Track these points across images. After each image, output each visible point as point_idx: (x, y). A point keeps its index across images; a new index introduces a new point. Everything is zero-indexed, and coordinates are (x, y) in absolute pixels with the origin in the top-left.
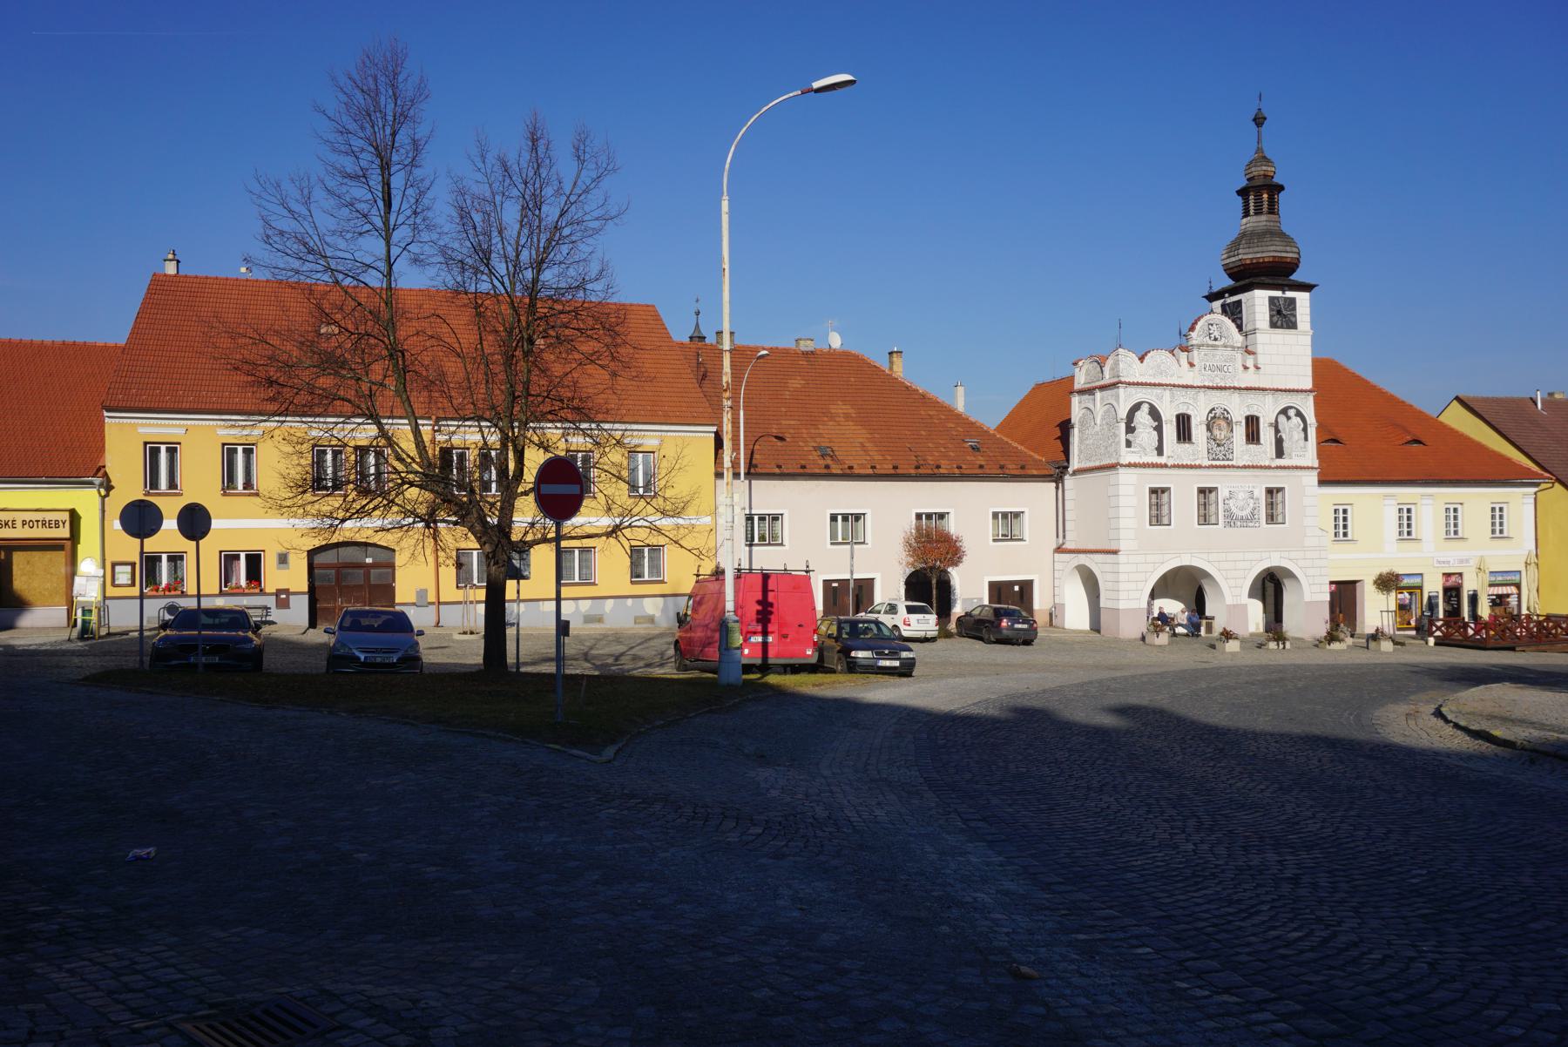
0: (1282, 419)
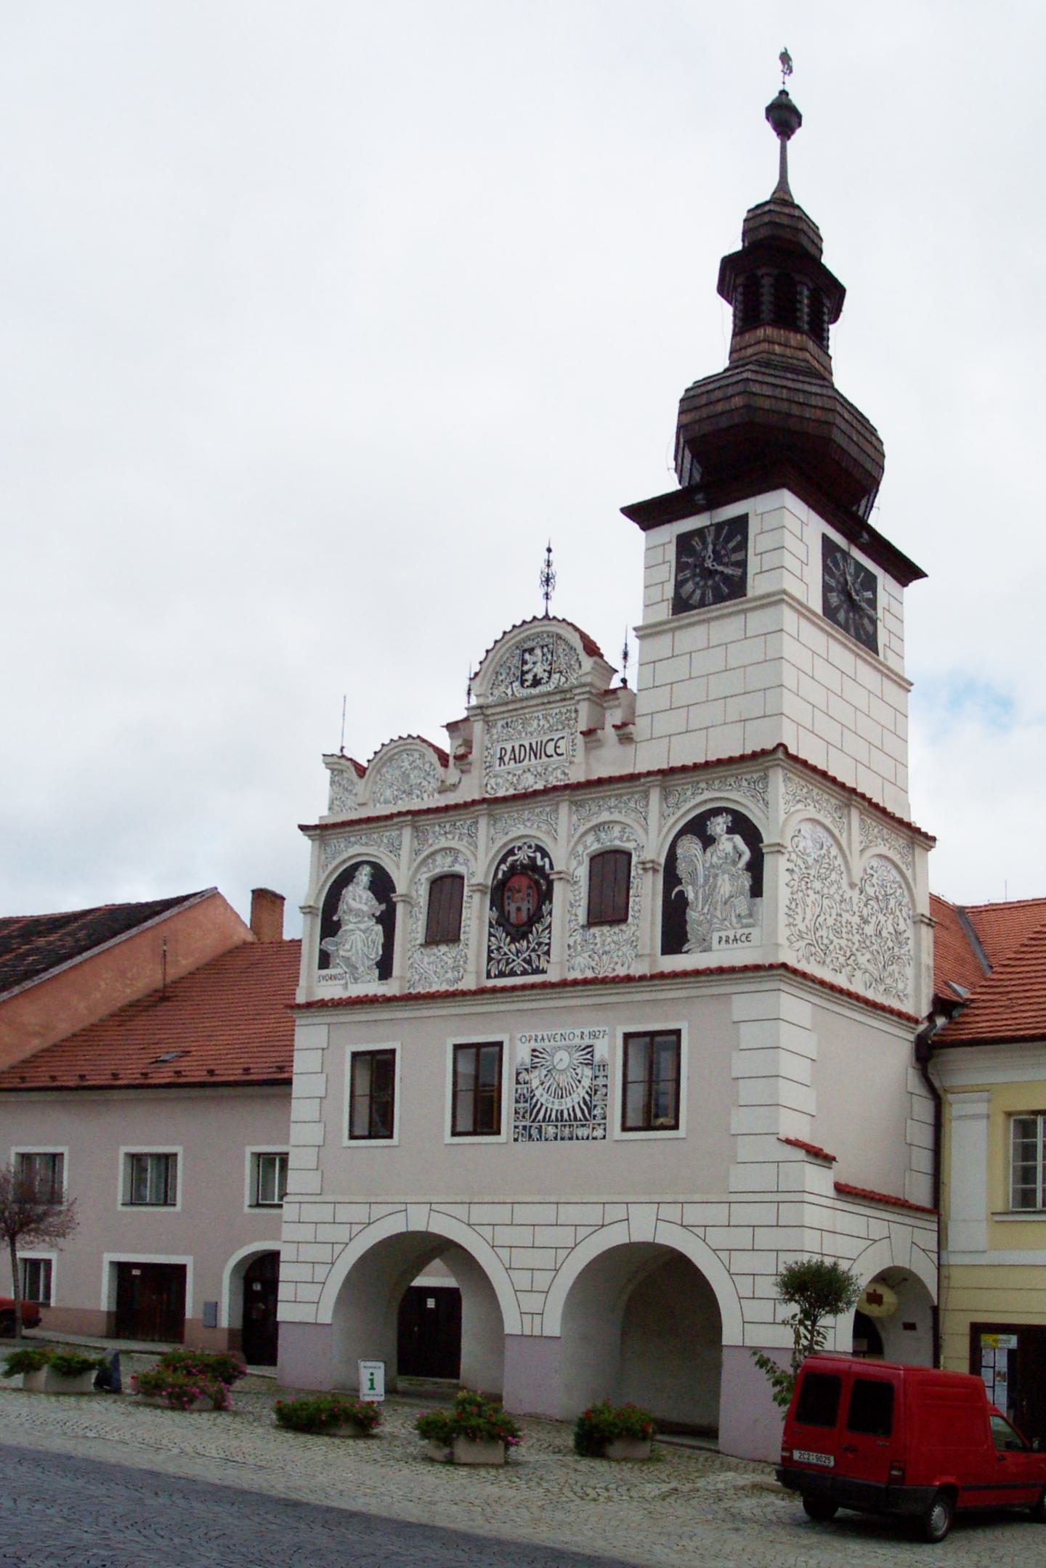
0: (690, 846)
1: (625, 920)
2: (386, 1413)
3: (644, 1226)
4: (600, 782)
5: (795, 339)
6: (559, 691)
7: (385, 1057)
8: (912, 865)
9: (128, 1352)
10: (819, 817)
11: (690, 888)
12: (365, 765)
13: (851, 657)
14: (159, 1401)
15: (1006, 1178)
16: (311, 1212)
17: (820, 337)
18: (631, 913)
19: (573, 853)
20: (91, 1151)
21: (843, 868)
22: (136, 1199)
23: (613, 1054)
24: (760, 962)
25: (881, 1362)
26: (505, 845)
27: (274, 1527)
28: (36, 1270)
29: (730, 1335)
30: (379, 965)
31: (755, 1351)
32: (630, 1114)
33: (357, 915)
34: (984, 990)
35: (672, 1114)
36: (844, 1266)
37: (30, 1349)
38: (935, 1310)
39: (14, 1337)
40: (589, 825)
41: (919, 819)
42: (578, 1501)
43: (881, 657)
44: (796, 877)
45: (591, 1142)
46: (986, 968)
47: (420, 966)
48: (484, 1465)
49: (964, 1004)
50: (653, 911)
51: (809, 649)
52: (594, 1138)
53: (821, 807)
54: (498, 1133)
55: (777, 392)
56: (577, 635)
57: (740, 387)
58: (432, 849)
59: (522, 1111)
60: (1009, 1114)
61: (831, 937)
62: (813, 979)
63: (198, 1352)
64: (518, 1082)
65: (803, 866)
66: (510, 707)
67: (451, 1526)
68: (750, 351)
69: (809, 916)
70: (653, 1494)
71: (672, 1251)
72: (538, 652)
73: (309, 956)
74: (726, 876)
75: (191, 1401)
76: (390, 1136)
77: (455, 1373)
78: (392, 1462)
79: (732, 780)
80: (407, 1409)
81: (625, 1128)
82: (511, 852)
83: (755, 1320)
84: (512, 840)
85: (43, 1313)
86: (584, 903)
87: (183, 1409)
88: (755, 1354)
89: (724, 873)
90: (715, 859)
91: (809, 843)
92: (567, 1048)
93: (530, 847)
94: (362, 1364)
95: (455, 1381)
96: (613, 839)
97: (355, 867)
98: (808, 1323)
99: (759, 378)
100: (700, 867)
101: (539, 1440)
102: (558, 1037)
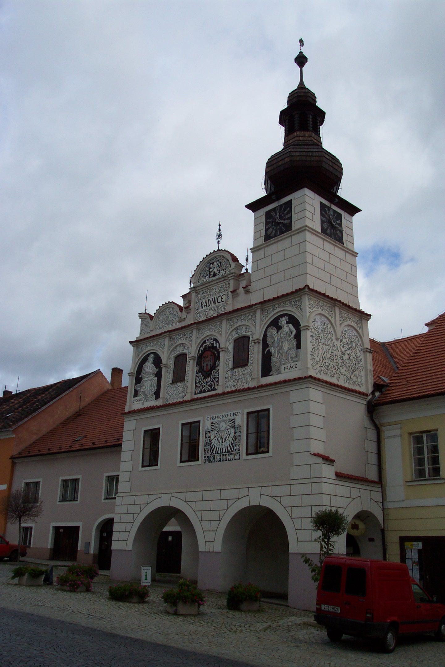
0: (273, 331)
1: (247, 365)
2: (151, 591)
3: (255, 498)
4: (238, 310)
5: (307, 134)
6: (223, 277)
7: (156, 431)
8: (362, 327)
9: (56, 566)
10: (323, 312)
11: (272, 348)
12: (153, 315)
13: (333, 247)
14: (66, 588)
15: (411, 464)
16: (127, 500)
17: (317, 132)
18: (249, 361)
19: (228, 340)
20: (48, 478)
21: (333, 332)
22: (64, 499)
23: (243, 422)
24: (301, 376)
25: (359, 558)
26: (202, 340)
27: (105, 647)
28: (27, 530)
29: (292, 548)
30: (155, 393)
31: (303, 555)
32: (249, 448)
33: (148, 374)
34: (395, 378)
35: (266, 446)
36: (341, 511)
37: (22, 566)
38: (383, 531)
39: (16, 561)
40: (234, 328)
41: (364, 307)
42: (228, 633)
43: (345, 245)
44: (314, 338)
45: (234, 461)
46: (395, 368)
47: (172, 392)
48: (190, 615)
49: (387, 385)
50: (258, 359)
51: (317, 248)
52: (235, 459)
53: (323, 309)
54: (198, 460)
55: (301, 154)
56: (229, 255)
57: (288, 155)
58: (176, 345)
59: (207, 450)
60: (410, 434)
61: (330, 362)
62: (323, 381)
63: (82, 565)
64: (206, 438)
65: (317, 334)
66: (205, 286)
67: (175, 645)
68: (291, 141)
69: (320, 354)
70: (260, 628)
71: (267, 509)
72: (215, 263)
73: (131, 392)
74: (286, 342)
75: (77, 588)
76: (157, 465)
77: (179, 571)
78: (152, 615)
79: (288, 302)
80: (159, 589)
81: (248, 454)
82: (205, 342)
83: (303, 540)
84: (205, 337)
85: (28, 550)
86: (232, 359)
87: (74, 591)
88: (303, 556)
89: (285, 340)
90: (282, 335)
91: (319, 324)
92: (225, 421)
93: (211, 339)
94: (143, 568)
95: (178, 575)
96: (243, 332)
97: (148, 355)
98: (326, 540)
99: (295, 150)
100: (276, 339)
101: (212, 602)
102: (221, 417)
